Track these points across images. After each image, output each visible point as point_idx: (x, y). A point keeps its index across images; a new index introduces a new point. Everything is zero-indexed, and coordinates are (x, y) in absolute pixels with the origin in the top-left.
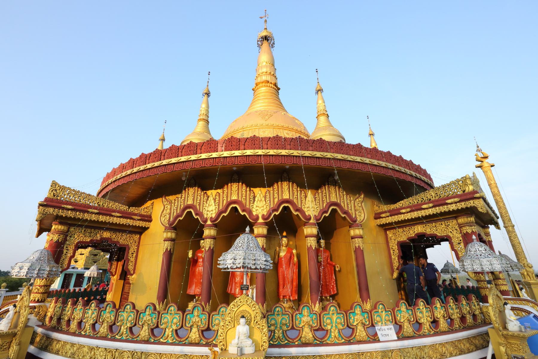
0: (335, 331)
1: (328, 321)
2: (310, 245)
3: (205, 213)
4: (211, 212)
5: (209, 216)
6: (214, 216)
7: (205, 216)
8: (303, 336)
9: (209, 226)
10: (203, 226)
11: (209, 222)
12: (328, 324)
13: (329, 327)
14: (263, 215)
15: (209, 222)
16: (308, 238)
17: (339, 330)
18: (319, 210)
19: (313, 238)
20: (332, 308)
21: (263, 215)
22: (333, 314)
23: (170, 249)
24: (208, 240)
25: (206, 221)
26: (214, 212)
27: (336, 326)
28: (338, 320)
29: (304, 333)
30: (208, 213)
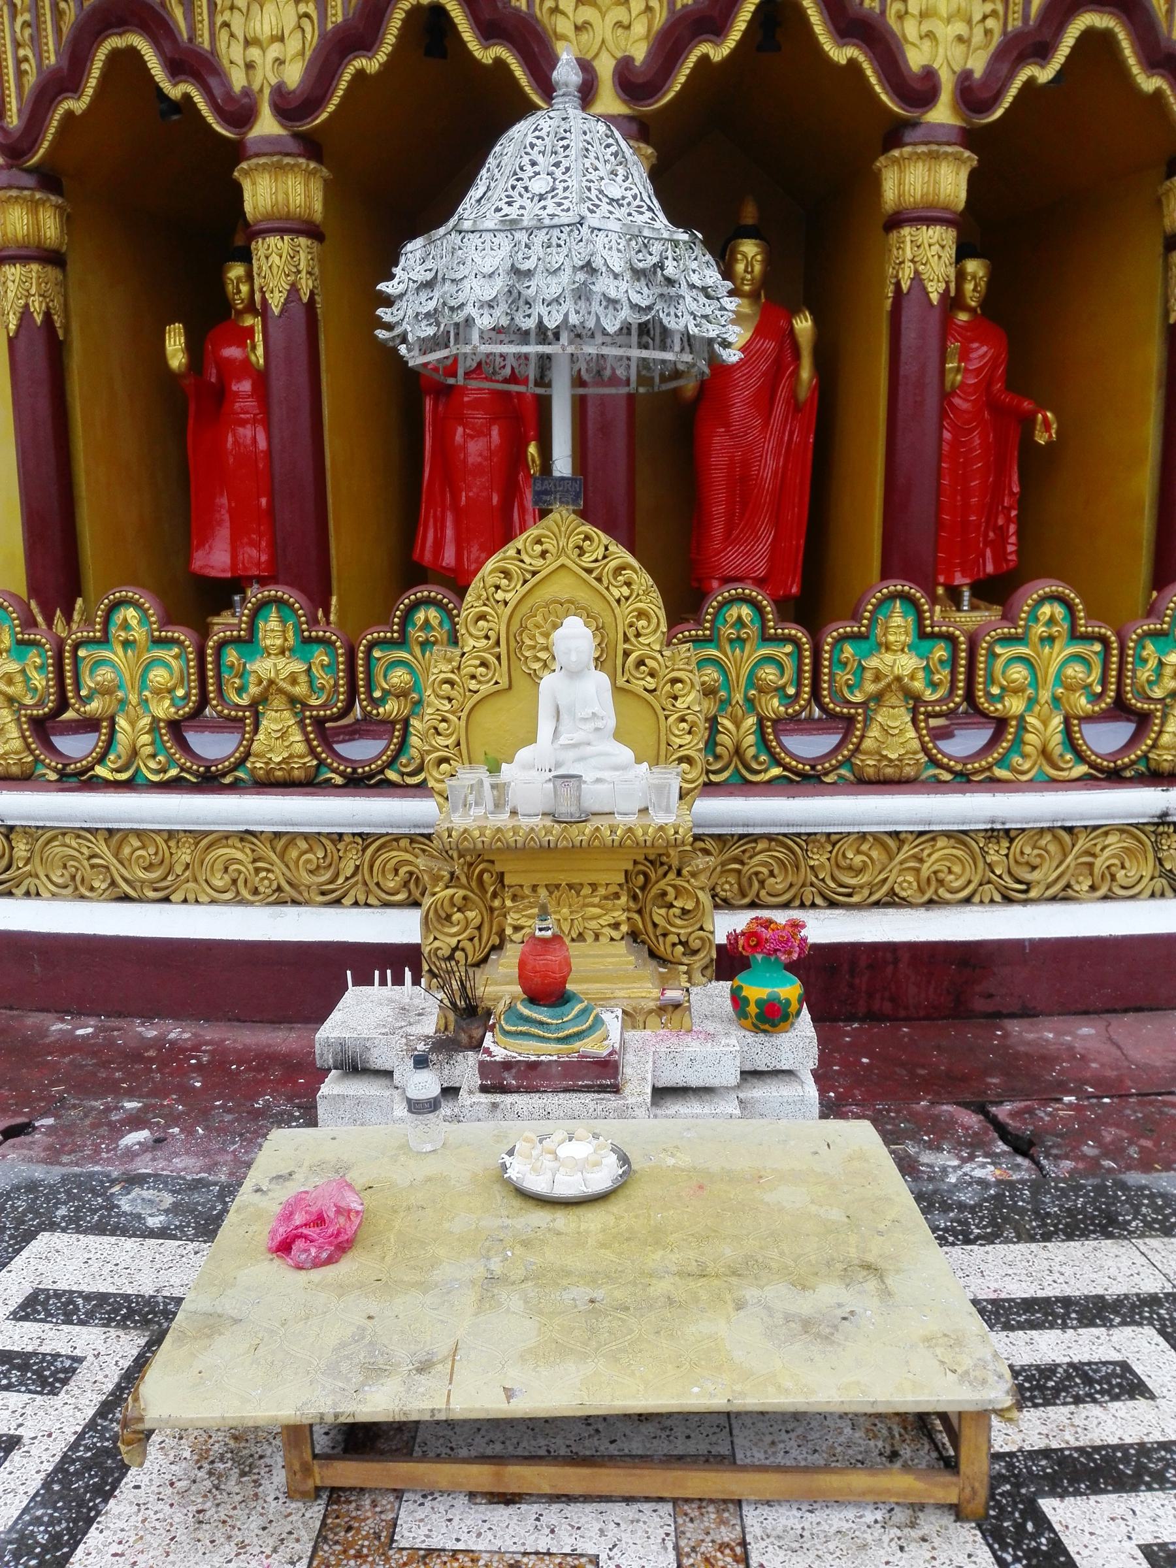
0: (1045, 723)
1: (1018, 673)
2: (917, 277)
3: (232, 54)
4: (274, 51)
5: (265, 77)
6: (293, 75)
7: (238, 79)
8: (868, 744)
9: (271, 147)
10: (236, 152)
11: (267, 125)
12: (1016, 691)
13: (1015, 705)
14: (624, 68)
15: (267, 125)
16: (906, 231)
17: (1067, 721)
18: (997, 39)
19: (935, 233)
20: (1046, 610)
21: (624, 68)
22: (1051, 639)
23: (48, 315)
24: (273, 241)
25: (241, 113)
26: (293, 44)
27: (1056, 699)
28: (1076, 671)
29: (874, 732)
30: (254, 53)
